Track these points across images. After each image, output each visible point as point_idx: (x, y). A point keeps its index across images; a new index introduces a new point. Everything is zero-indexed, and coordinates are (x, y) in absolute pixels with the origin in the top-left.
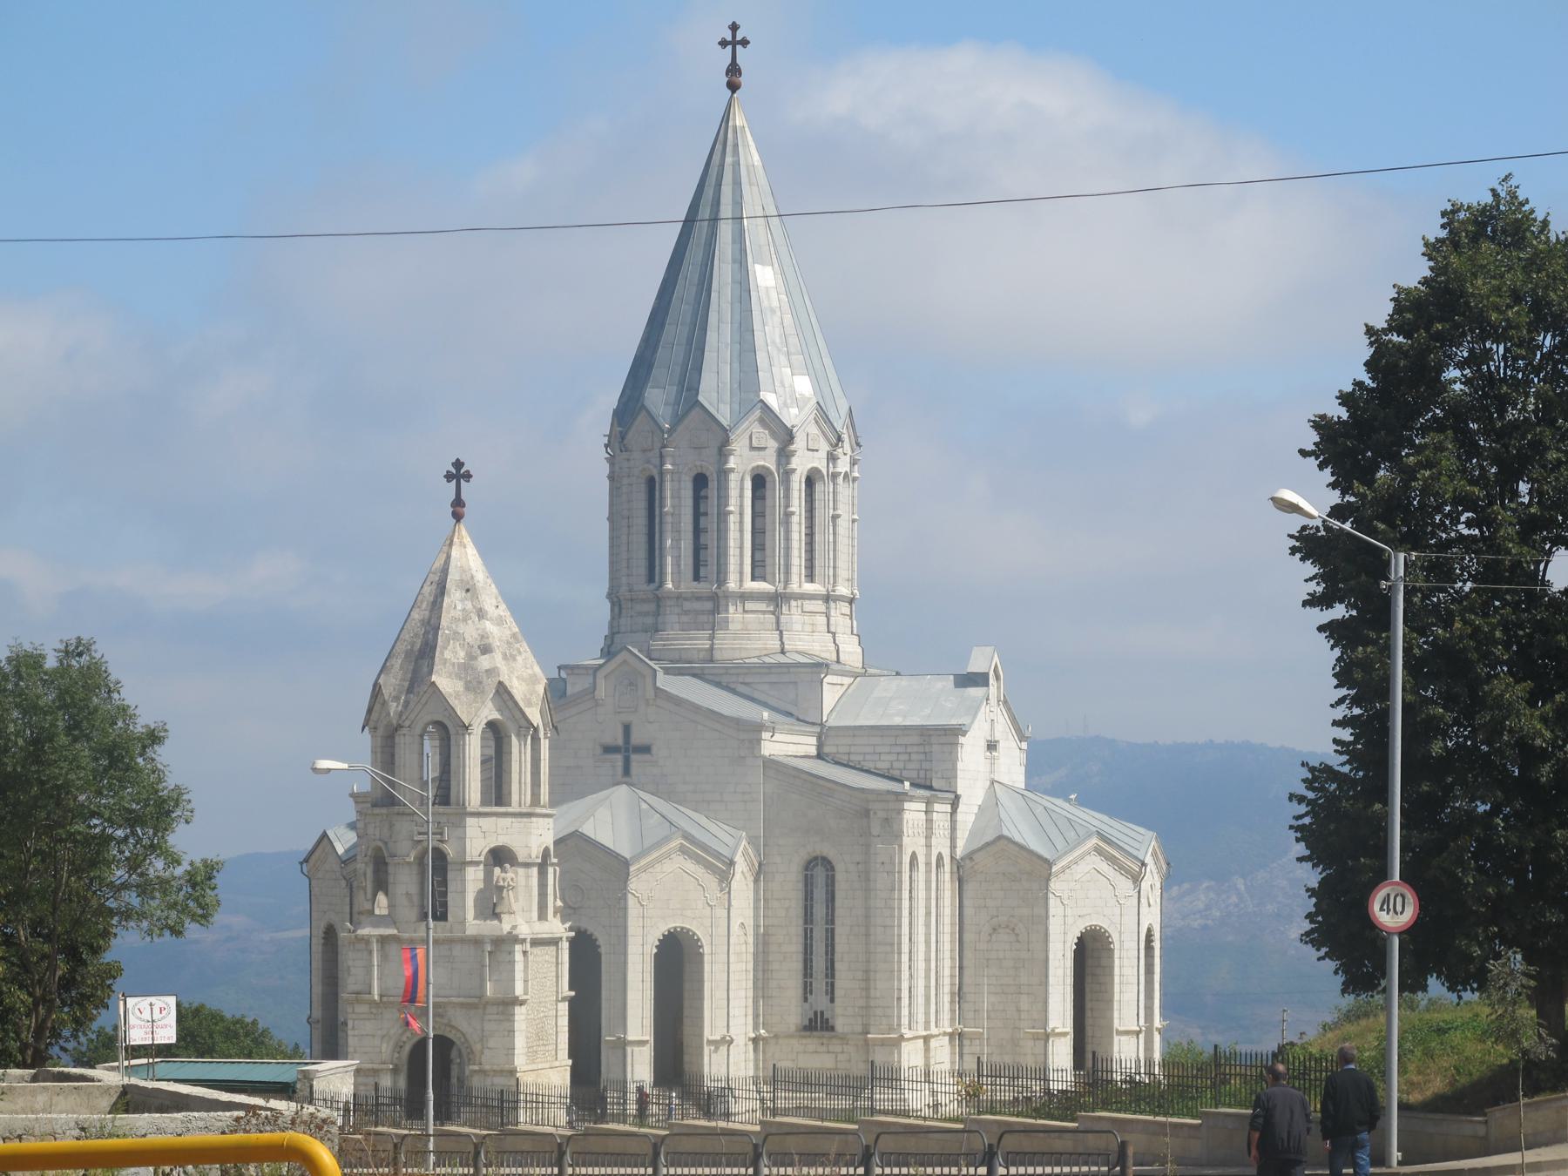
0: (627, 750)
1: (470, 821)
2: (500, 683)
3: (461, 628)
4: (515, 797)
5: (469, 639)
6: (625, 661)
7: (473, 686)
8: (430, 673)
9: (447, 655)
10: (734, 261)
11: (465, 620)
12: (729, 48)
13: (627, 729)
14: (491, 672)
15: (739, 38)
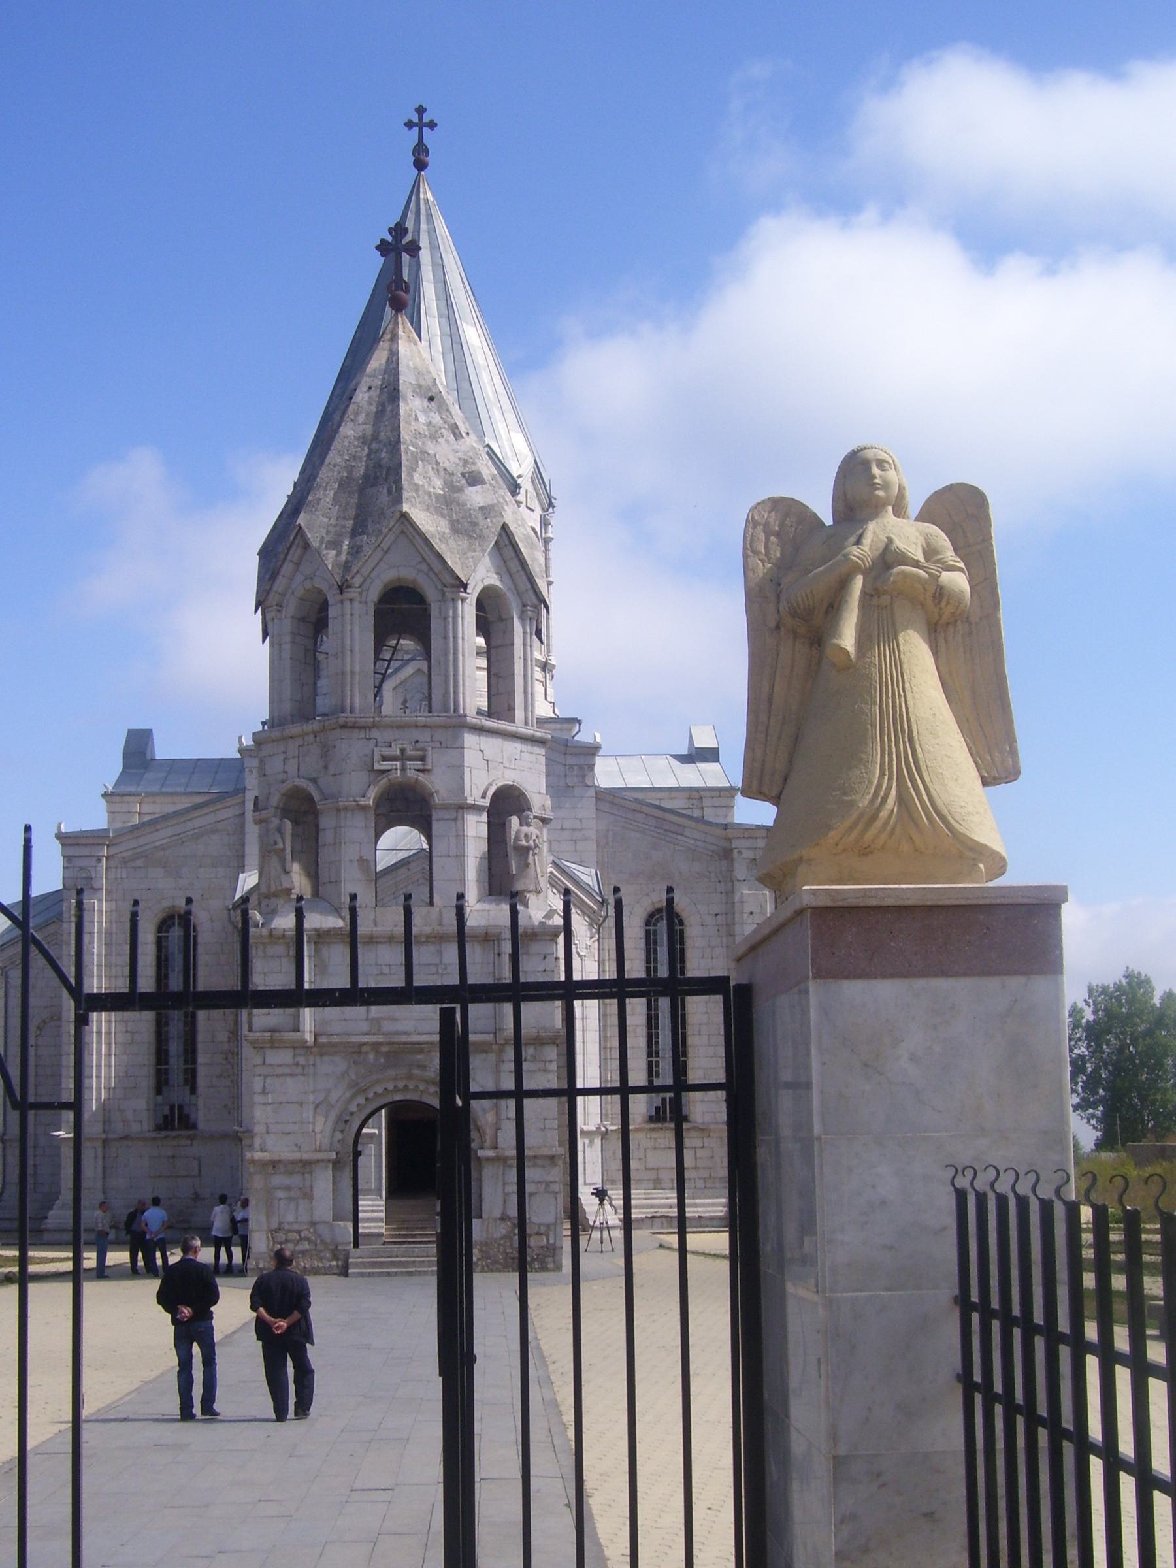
1: (470, 740)
2: (505, 527)
3: (431, 448)
4: (519, 714)
5: (447, 465)
7: (465, 526)
8: (399, 500)
9: (418, 479)
10: (440, 315)
11: (434, 437)
12: (416, 129)
14: (486, 510)
15: (426, 119)
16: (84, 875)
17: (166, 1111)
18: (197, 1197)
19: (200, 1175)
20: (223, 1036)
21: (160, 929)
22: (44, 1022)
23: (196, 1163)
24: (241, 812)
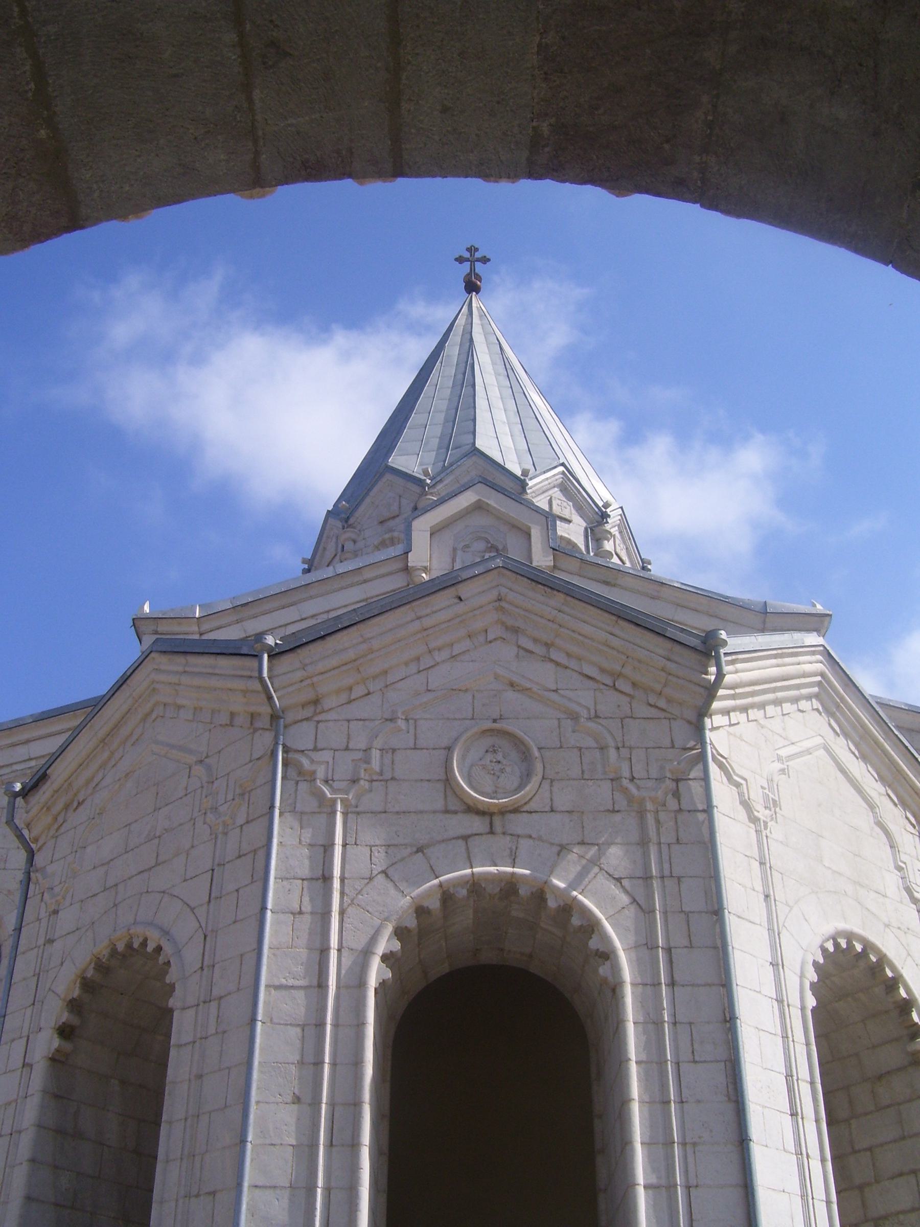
6: (479, 507)
15: (478, 255)
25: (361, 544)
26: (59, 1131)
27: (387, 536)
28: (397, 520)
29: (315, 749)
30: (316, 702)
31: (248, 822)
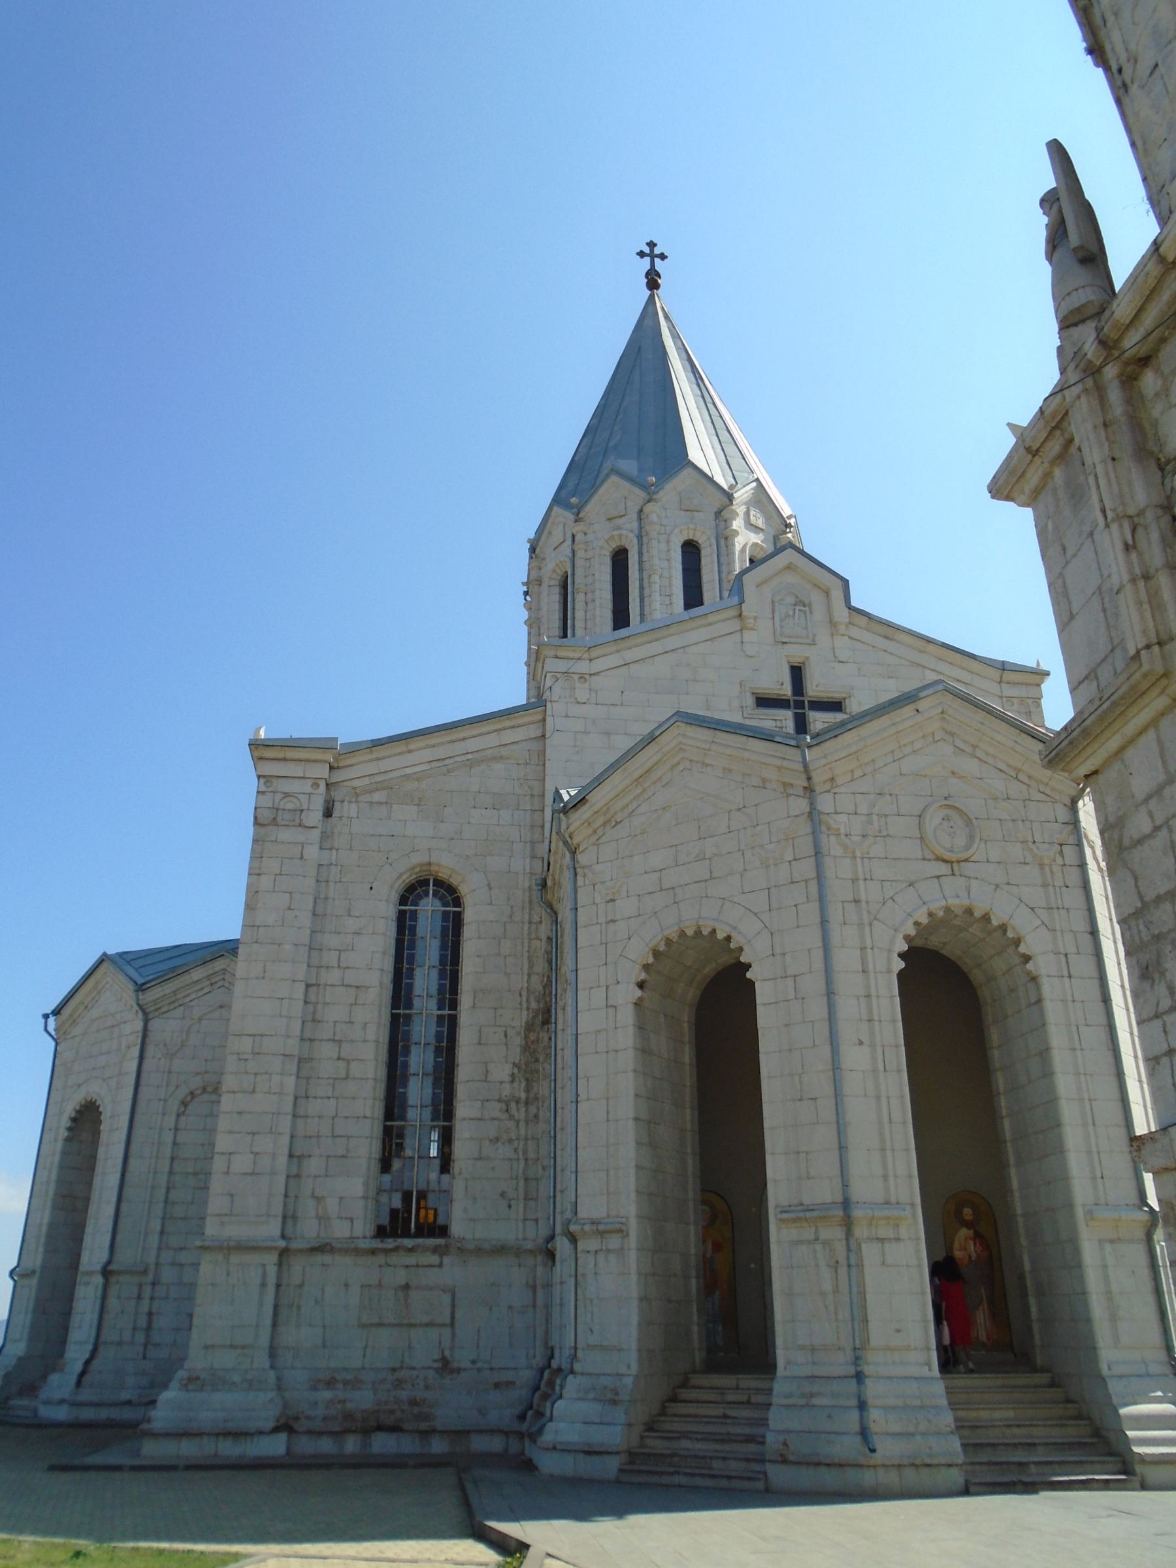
0: (800, 705)
6: (789, 567)
12: (648, 259)
13: (797, 673)
15: (657, 251)
16: (289, 806)
17: (397, 1203)
18: (445, 1366)
19: (452, 1324)
20: (501, 1072)
21: (403, 900)
22: (192, 1093)
23: (446, 1299)
24: (539, 733)
25: (590, 537)
26: (643, 1051)
27: (615, 533)
28: (623, 519)
29: (836, 813)
30: (832, 779)
31: (795, 860)
